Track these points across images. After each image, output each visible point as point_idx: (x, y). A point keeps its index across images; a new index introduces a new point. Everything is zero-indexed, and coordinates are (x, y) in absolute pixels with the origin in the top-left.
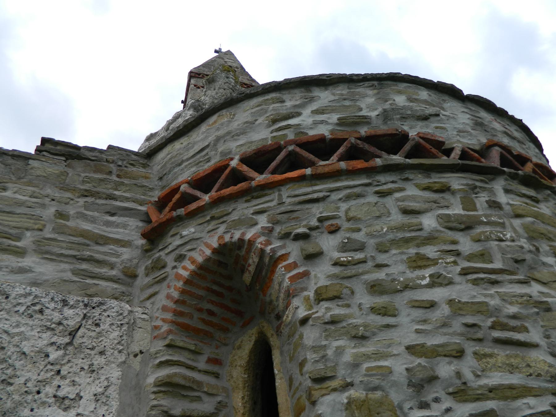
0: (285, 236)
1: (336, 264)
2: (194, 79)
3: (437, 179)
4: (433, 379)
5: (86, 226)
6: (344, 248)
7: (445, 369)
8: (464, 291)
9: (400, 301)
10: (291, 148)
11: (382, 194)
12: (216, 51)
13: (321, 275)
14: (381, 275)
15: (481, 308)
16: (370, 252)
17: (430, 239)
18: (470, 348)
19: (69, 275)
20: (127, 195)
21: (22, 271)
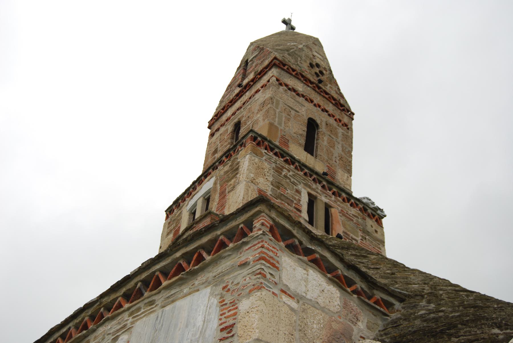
2: (278, 70)
12: (284, 22)
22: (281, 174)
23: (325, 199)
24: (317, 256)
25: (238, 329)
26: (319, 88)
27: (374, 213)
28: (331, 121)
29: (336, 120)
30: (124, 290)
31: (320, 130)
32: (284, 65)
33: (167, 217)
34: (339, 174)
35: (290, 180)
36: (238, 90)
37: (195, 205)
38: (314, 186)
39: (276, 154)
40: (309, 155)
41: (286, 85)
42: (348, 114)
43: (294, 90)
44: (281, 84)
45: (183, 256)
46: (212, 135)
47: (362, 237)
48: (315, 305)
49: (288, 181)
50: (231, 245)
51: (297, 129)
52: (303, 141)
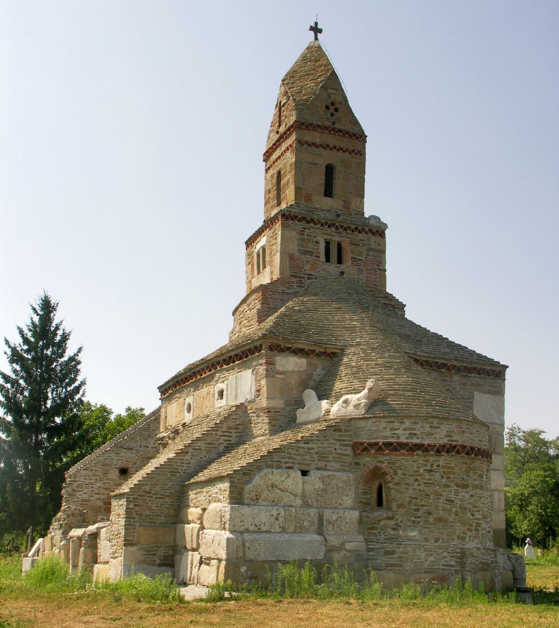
0: (391, 468)
1: (401, 478)
3: (427, 458)
4: (412, 502)
5: (340, 452)
6: (403, 474)
7: (414, 501)
8: (422, 487)
9: (410, 487)
10: (395, 444)
11: (414, 461)
13: (397, 479)
14: (408, 482)
15: (423, 491)
16: (407, 476)
17: (420, 475)
18: (420, 498)
19: (340, 467)
20: (347, 439)
21: (333, 466)
22: (303, 234)
23: (337, 239)
24: (294, 348)
25: (261, 392)
26: (333, 129)
27: (377, 229)
28: (347, 155)
29: (350, 153)
30: (222, 358)
31: (337, 170)
32: (303, 124)
33: (247, 249)
34: (353, 203)
35: (310, 236)
36: (276, 137)
37: (259, 250)
38: (329, 231)
39: (300, 220)
40: (328, 199)
41: (307, 143)
42: (361, 140)
43: (313, 144)
44: (302, 144)
45: (241, 352)
46: (267, 171)
47: (367, 255)
48: (292, 372)
49: (309, 237)
50: (256, 354)
51: (318, 180)
52: (322, 190)
